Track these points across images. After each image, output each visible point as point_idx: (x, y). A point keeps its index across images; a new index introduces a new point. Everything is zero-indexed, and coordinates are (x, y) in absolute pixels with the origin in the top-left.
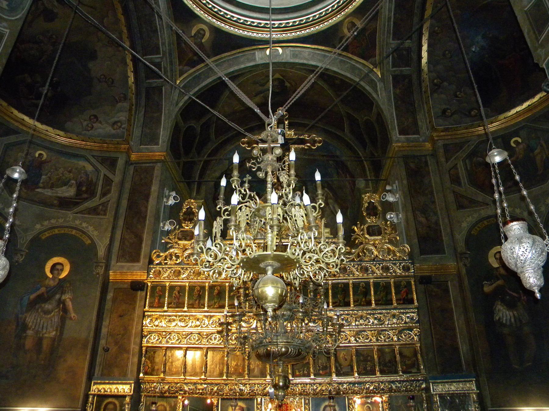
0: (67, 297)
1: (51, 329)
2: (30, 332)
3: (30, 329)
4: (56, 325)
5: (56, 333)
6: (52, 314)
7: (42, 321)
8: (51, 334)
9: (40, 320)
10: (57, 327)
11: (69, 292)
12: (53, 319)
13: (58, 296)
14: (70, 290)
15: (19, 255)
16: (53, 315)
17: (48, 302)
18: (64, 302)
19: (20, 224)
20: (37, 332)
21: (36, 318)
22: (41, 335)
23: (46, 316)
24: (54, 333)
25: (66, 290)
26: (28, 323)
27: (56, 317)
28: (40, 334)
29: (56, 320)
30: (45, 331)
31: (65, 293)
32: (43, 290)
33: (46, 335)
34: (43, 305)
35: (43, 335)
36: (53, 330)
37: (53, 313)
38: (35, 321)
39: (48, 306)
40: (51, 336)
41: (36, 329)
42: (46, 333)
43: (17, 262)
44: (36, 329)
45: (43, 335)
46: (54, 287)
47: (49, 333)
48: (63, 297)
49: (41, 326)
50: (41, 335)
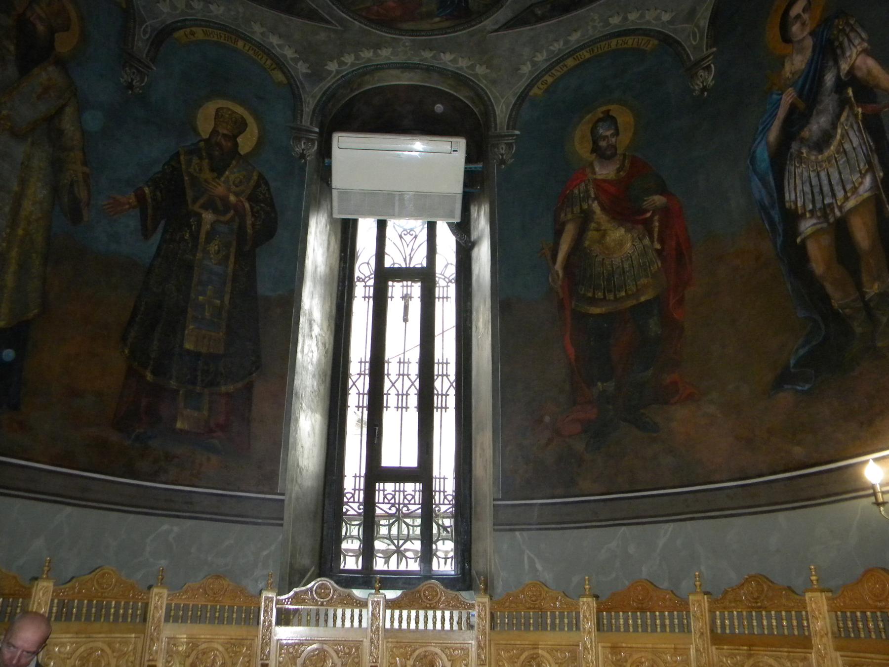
0: (854, 56)
1: (856, 177)
2: (807, 226)
3: (803, 216)
4: (861, 156)
5: (874, 179)
6: (838, 137)
7: (823, 175)
8: (861, 190)
9: (818, 175)
10: (869, 163)
11: (852, 35)
12: (847, 146)
13: (829, 79)
14: (853, 30)
15: (701, 73)
16: (842, 136)
17: (815, 112)
18: (853, 78)
19: (674, 14)
20: (826, 210)
21: (805, 174)
22: (838, 213)
23: (826, 154)
24: (868, 180)
25: (841, 44)
26: (793, 207)
27: (851, 133)
28: (832, 210)
29: (855, 144)
30: (840, 194)
31: (843, 53)
32: (788, 97)
33: (851, 204)
34: (805, 133)
35: (840, 208)
36: (863, 176)
37: (839, 131)
38: (807, 189)
39: (818, 124)
40: (866, 195)
41: (819, 205)
42: (846, 199)
43: (704, 89)
44: (819, 205)
45: (840, 208)
46: (810, 63)
47: (855, 190)
48: (845, 67)
49: (826, 188)
50: (838, 213)
